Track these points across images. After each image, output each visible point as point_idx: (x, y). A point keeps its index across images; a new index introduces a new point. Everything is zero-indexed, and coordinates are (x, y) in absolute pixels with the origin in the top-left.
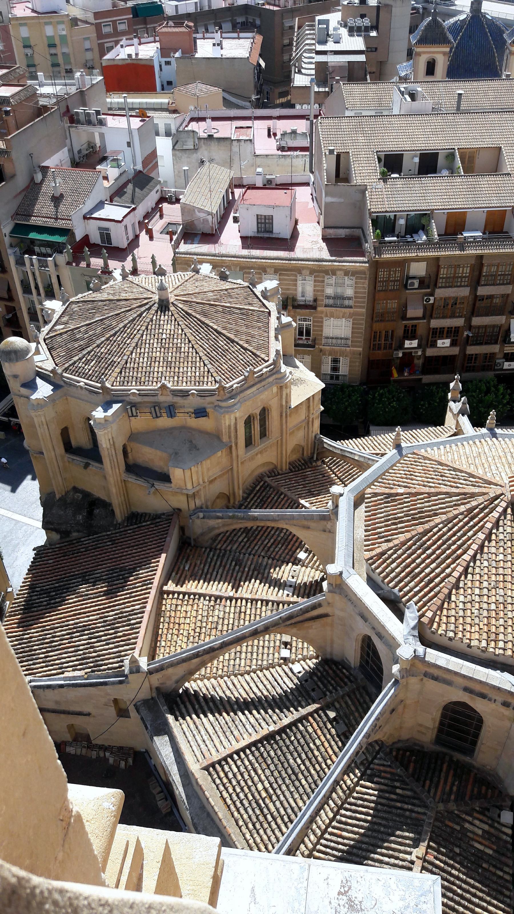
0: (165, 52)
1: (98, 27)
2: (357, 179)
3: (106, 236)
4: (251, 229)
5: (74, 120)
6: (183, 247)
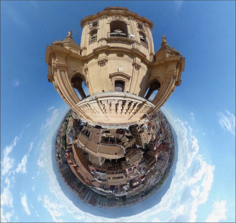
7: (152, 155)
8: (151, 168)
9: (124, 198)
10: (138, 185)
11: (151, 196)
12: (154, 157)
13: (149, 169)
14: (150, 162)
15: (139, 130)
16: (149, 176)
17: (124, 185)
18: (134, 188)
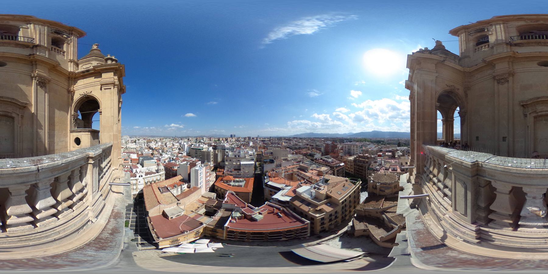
0: (383, 154)
1: (376, 152)
2: (403, 165)
3: (377, 169)
4: (392, 169)
5: (375, 159)
6: (385, 171)
7: (353, 164)
8: (369, 156)
9: (399, 145)
10: (387, 151)
11: (377, 138)
12: (354, 160)
13: (371, 158)
14: (364, 162)
15: (328, 209)
16: (372, 152)
17: (401, 156)
18: (391, 151)
